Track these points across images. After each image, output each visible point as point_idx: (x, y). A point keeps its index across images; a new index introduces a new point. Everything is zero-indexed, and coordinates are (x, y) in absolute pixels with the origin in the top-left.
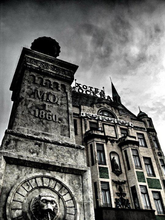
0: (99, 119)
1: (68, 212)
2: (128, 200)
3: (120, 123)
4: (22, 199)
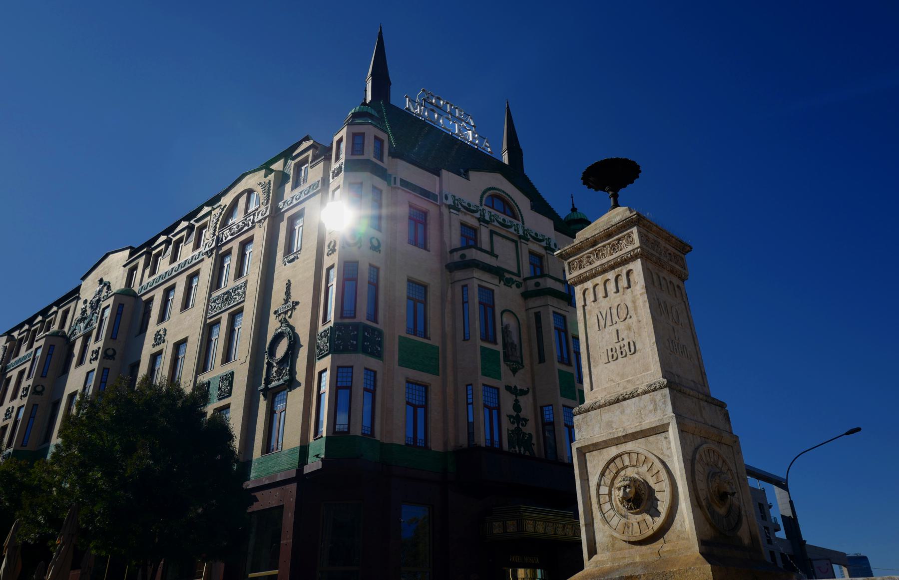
0: (484, 216)
3: (529, 237)
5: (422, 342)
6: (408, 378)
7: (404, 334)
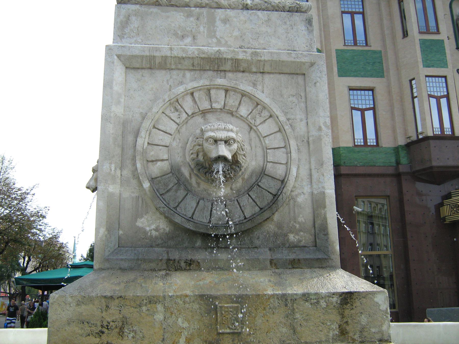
1: (270, 158)
4: (167, 140)
5: (362, 50)
6: (349, 87)
7: (341, 46)
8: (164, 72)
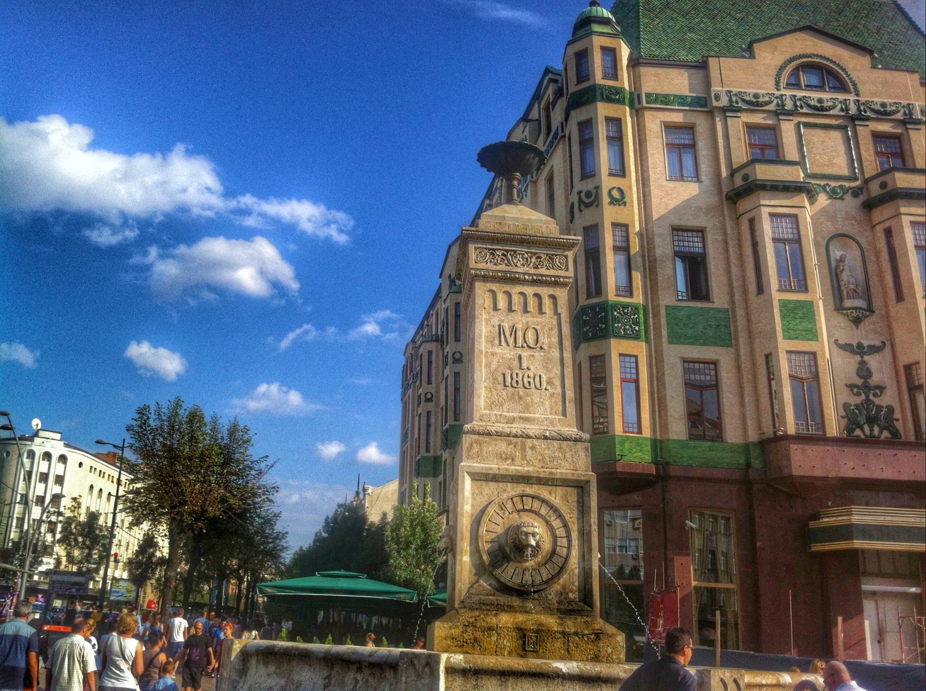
2: (891, 409)
8: (494, 483)
